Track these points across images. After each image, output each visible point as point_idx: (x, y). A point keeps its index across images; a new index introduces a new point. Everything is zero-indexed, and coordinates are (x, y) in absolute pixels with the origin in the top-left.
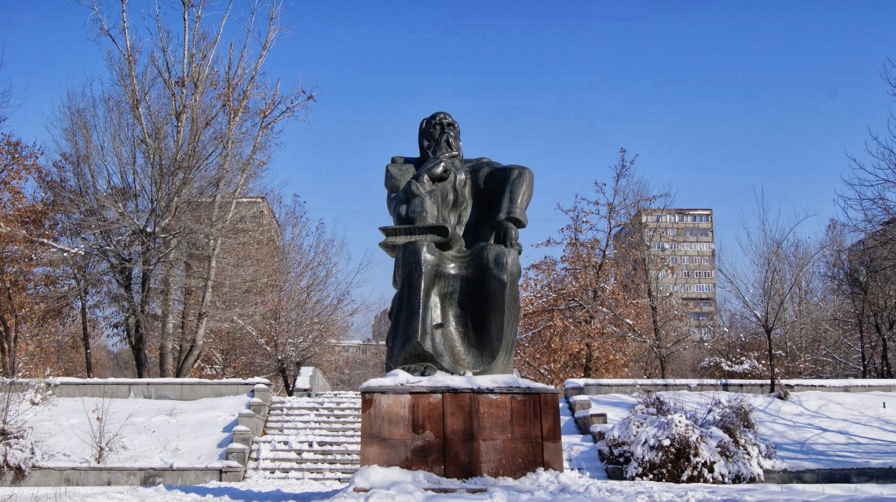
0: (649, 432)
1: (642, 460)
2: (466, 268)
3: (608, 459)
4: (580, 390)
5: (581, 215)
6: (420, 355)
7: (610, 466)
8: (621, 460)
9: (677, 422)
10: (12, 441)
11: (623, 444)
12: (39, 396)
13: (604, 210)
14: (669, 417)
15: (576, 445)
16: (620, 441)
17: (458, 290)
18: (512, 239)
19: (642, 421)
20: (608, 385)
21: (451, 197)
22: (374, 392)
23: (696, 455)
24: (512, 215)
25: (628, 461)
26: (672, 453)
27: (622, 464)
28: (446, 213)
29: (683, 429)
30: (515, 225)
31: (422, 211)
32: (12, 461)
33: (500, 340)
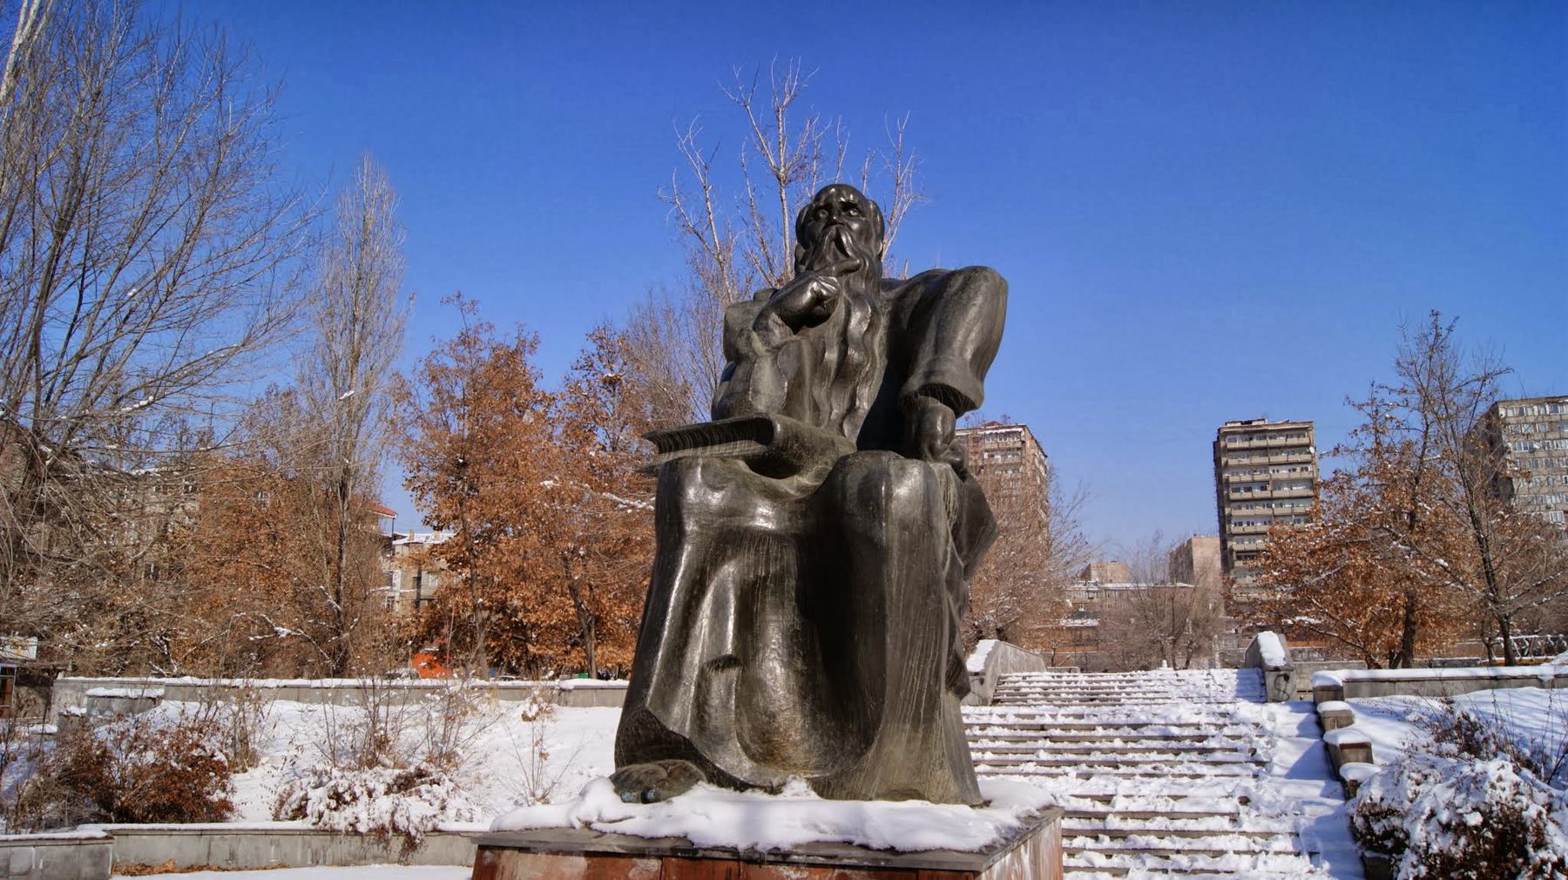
0: (1437, 795)
1: (1426, 851)
2: (804, 515)
3: (1363, 836)
4: (1335, 692)
5: (1382, 410)
6: (658, 740)
7: (1368, 854)
8: (1389, 844)
9: (1493, 779)
10: (423, 788)
11: (1391, 812)
12: (535, 708)
13: (1415, 399)
14: (1479, 766)
15: (1310, 803)
16: (1385, 806)
17: (794, 569)
18: (934, 436)
19: (1427, 771)
20: (1389, 681)
21: (832, 356)
22: (504, 848)
23: (1540, 845)
24: (936, 379)
25: (1400, 846)
26: (1487, 840)
27: (1390, 852)
28: (820, 393)
29: (1507, 795)
30: (947, 402)
31: (746, 391)
32: (402, 823)
33: (880, 695)
